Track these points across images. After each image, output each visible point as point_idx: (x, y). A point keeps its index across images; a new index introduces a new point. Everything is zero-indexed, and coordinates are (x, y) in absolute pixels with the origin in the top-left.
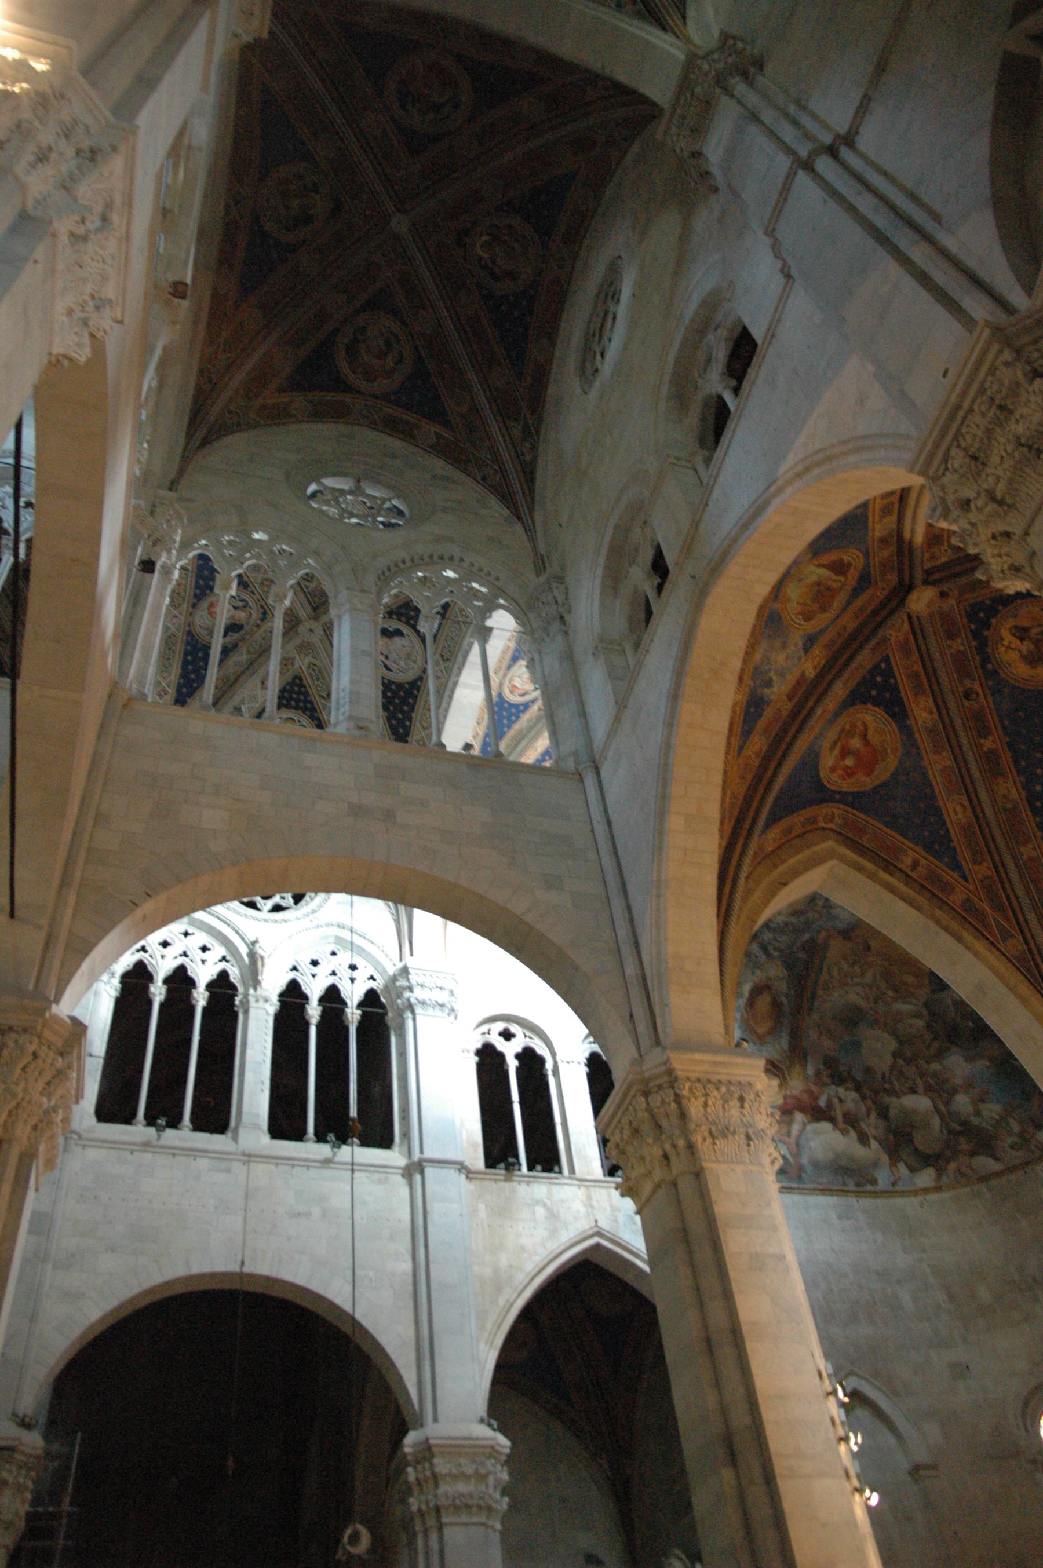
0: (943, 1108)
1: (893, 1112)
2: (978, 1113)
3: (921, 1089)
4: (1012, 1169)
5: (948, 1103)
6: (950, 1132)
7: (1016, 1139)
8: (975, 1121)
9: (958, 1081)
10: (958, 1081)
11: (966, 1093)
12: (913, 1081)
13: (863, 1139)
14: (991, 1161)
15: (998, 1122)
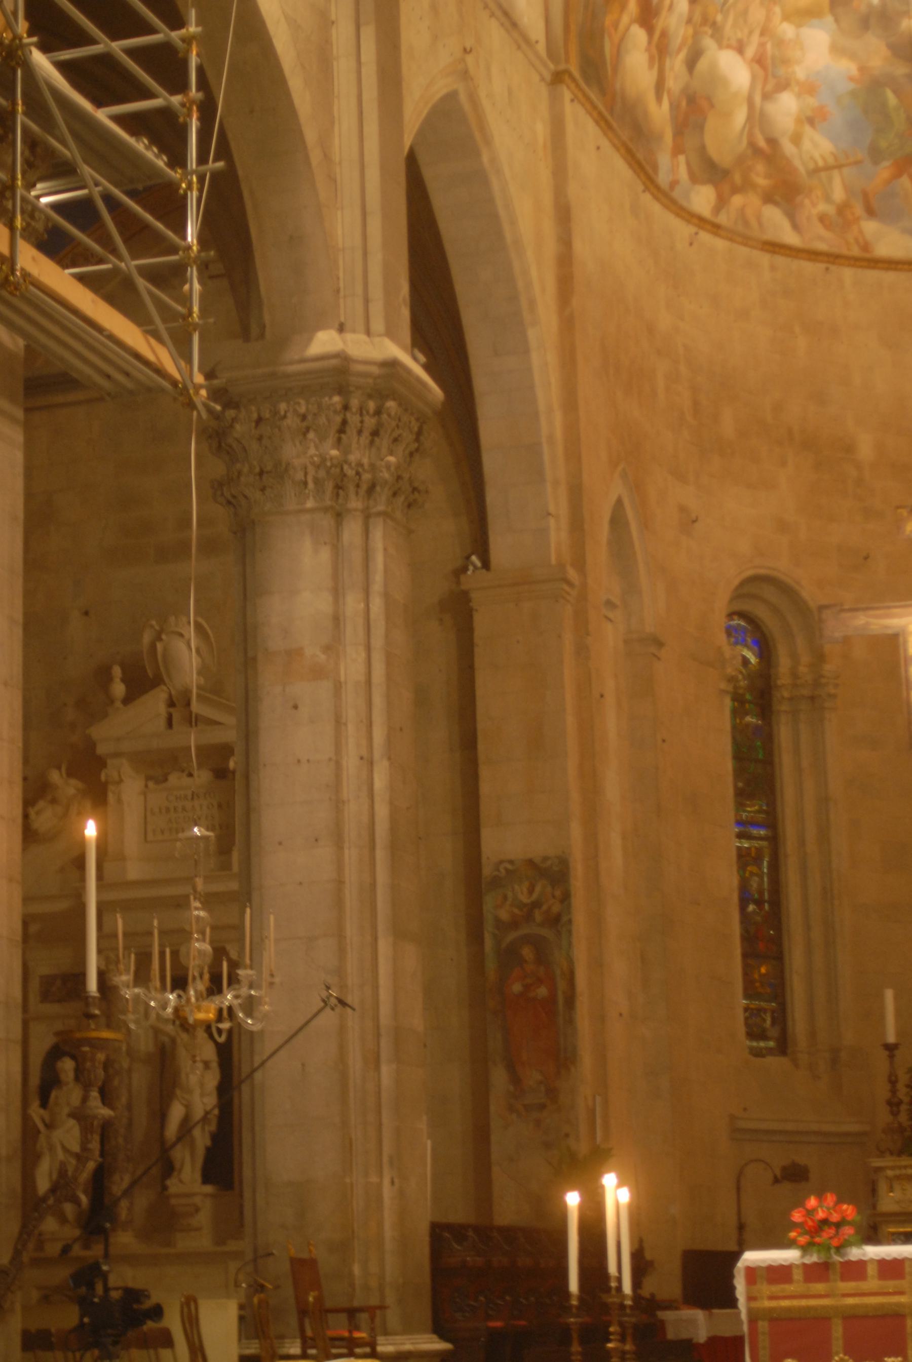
0: (758, 99)
1: (702, 65)
2: (797, 139)
3: (750, 51)
4: (813, 255)
5: (766, 97)
6: (752, 145)
7: (830, 209)
8: (788, 148)
9: (800, 72)
10: (800, 72)
11: (799, 95)
12: (751, 33)
13: (660, 86)
14: (786, 224)
15: (817, 171)
